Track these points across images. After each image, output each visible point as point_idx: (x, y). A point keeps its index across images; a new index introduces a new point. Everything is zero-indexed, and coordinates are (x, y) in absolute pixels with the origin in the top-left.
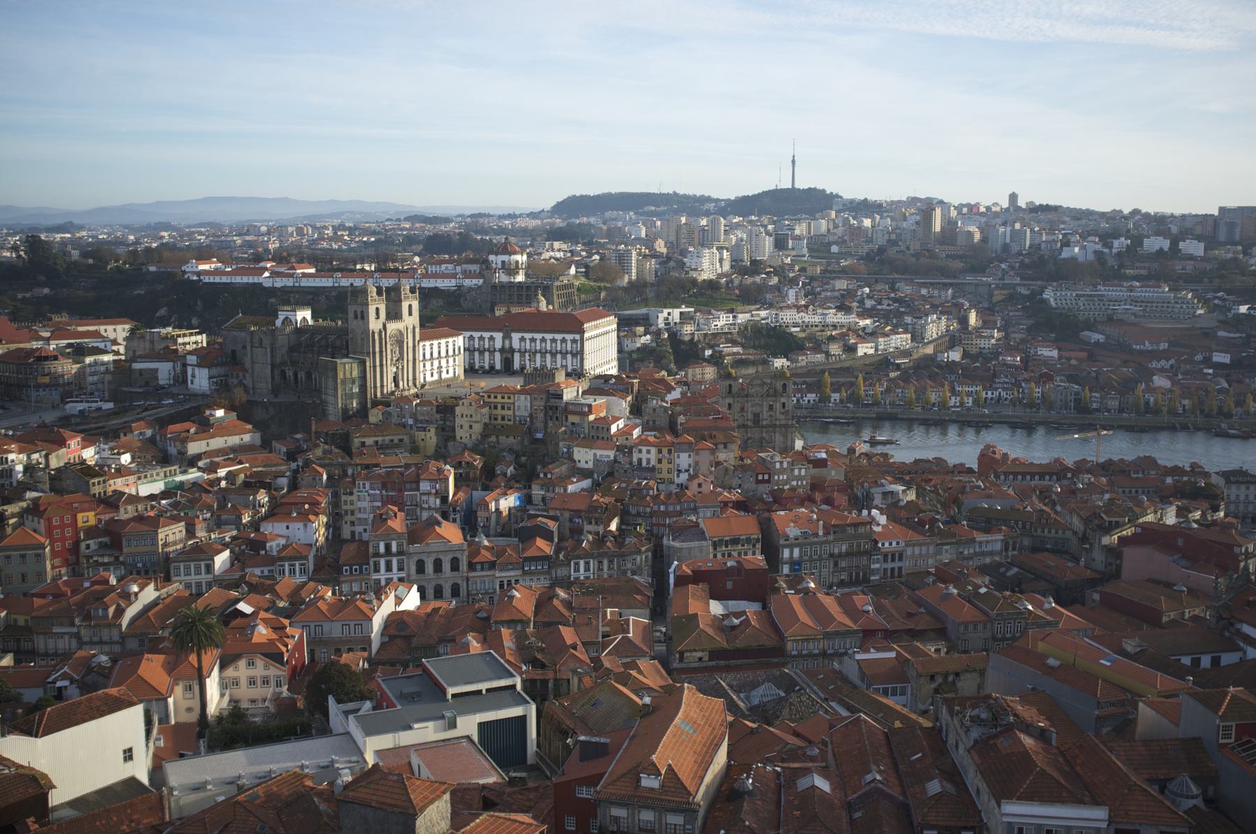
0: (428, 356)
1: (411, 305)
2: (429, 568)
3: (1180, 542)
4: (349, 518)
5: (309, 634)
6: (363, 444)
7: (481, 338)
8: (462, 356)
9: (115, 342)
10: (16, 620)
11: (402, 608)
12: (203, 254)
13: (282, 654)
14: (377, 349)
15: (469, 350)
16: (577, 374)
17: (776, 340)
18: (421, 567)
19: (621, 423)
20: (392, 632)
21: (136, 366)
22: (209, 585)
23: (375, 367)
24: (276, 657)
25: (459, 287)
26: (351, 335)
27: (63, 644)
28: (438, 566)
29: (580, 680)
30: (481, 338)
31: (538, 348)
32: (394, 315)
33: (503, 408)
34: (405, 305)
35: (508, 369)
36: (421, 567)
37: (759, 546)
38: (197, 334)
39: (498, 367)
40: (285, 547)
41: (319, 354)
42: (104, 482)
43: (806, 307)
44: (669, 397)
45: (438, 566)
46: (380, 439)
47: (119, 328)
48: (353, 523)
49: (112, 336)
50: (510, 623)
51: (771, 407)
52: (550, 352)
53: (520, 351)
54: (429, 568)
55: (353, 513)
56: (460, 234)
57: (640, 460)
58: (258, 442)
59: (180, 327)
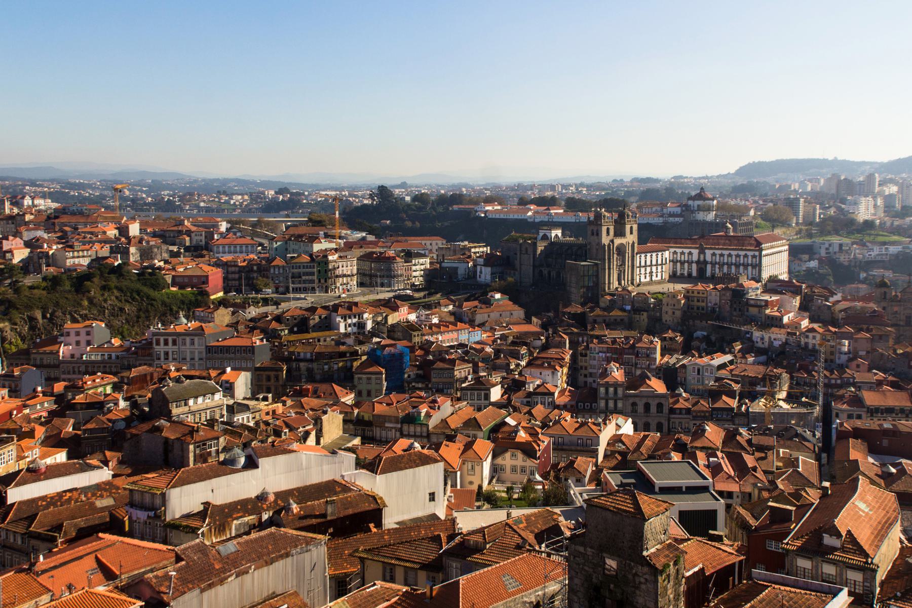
2: (641, 409)
4: (583, 372)
5: (554, 444)
10: (363, 417)
11: (620, 432)
12: (489, 200)
15: (674, 262)
16: (758, 280)
19: (791, 315)
25: (665, 223)
28: (647, 407)
29: (760, 492)
30: (682, 253)
32: (620, 233)
33: (698, 301)
34: (628, 227)
35: (702, 276)
39: (694, 274)
44: (831, 299)
47: (434, 243)
48: (585, 376)
49: (429, 247)
50: (702, 449)
53: (711, 263)
55: (586, 368)
56: (667, 189)
57: (806, 344)
59: (473, 242)
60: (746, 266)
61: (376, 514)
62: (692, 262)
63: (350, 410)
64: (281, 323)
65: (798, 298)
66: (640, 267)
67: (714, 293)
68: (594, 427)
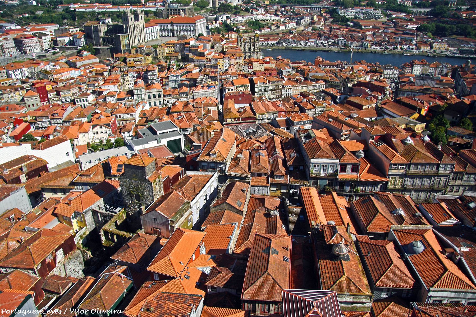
0: (148, 32)
1: (142, 16)
2: (152, 97)
3: (370, 86)
4: (127, 83)
6: (130, 60)
11: (144, 109)
14: (132, 31)
17: (257, 25)
18: (149, 97)
20: (142, 116)
21: (58, 39)
24: (108, 125)
27: (47, 124)
28: (154, 96)
32: (136, 18)
34: (140, 17)
36: (149, 97)
37: (249, 87)
40: (109, 92)
43: (265, 14)
44: (222, 43)
46: (135, 59)
51: (253, 45)
54: (152, 97)
58: (98, 61)
59: (71, 26)
61: (45, 168)
65: (210, 44)
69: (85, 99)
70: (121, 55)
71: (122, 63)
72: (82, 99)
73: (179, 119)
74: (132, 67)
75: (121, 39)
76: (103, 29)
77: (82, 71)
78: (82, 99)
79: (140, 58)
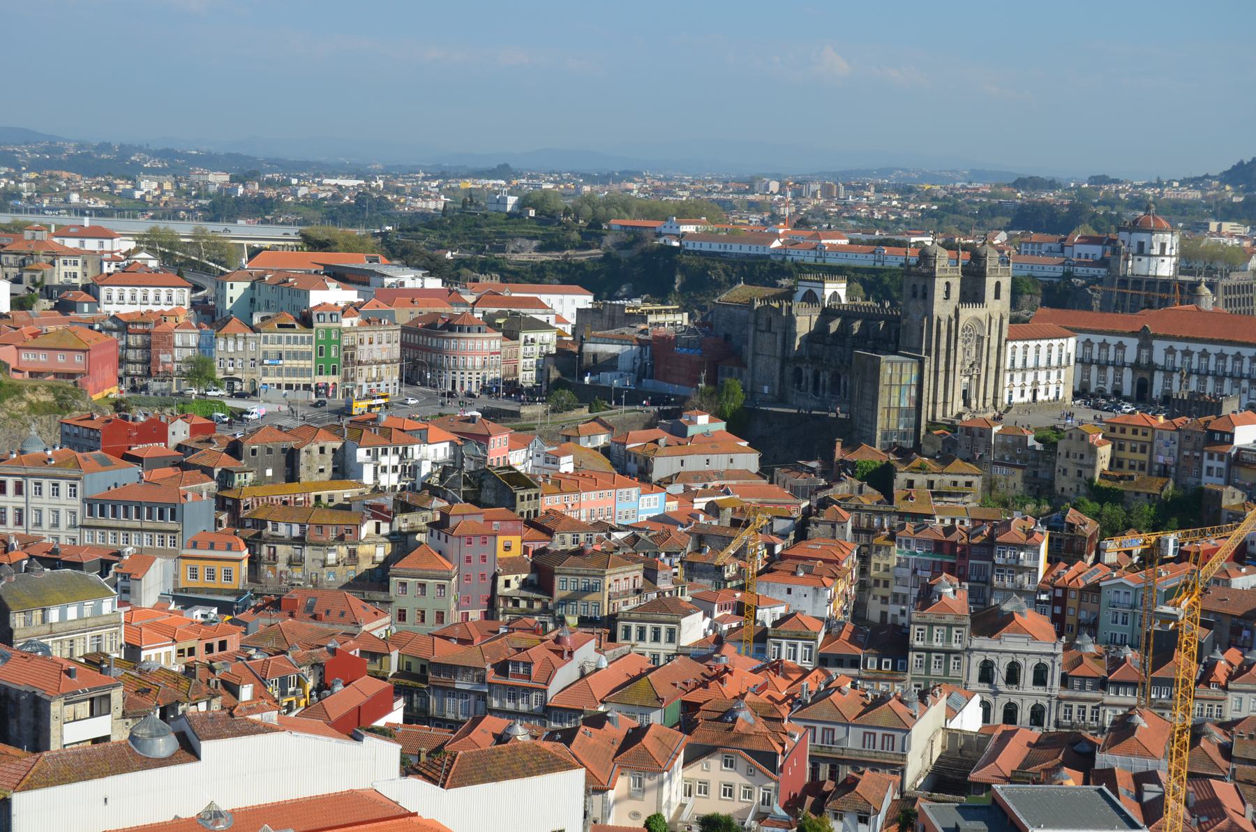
0: (1019, 364)
4: (880, 591)
6: (911, 484)
7: (1104, 345)
8: (1071, 370)
9: (560, 319)
12: (685, 213)
13: (776, 754)
14: (943, 346)
15: (1083, 362)
18: (986, 674)
22: (669, 658)
23: (936, 372)
26: (904, 322)
30: (1104, 345)
31: (1195, 366)
32: (972, 293)
33: (1133, 450)
34: (990, 283)
38: (675, 311)
39: (1127, 390)
40: (785, 618)
41: (855, 347)
42: (536, 496)
45: (1013, 675)
46: (936, 478)
48: (884, 600)
49: (558, 310)
52: (1215, 375)
55: (886, 584)
59: (653, 303)
60: (1237, 378)
62: (1124, 365)
63: (382, 650)
64: (239, 458)
66: (1013, 369)
67: (1167, 436)
68: (900, 709)
69: (663, 628)
70: (871, 455)
71: (867, 489)
72: (649, 628)
73: (1147, 797)
74: (915, 516)
75: (884, 379)
76: (805, 323)
77: (670, 497)
78: (649, 628)
79: (961, 480)
